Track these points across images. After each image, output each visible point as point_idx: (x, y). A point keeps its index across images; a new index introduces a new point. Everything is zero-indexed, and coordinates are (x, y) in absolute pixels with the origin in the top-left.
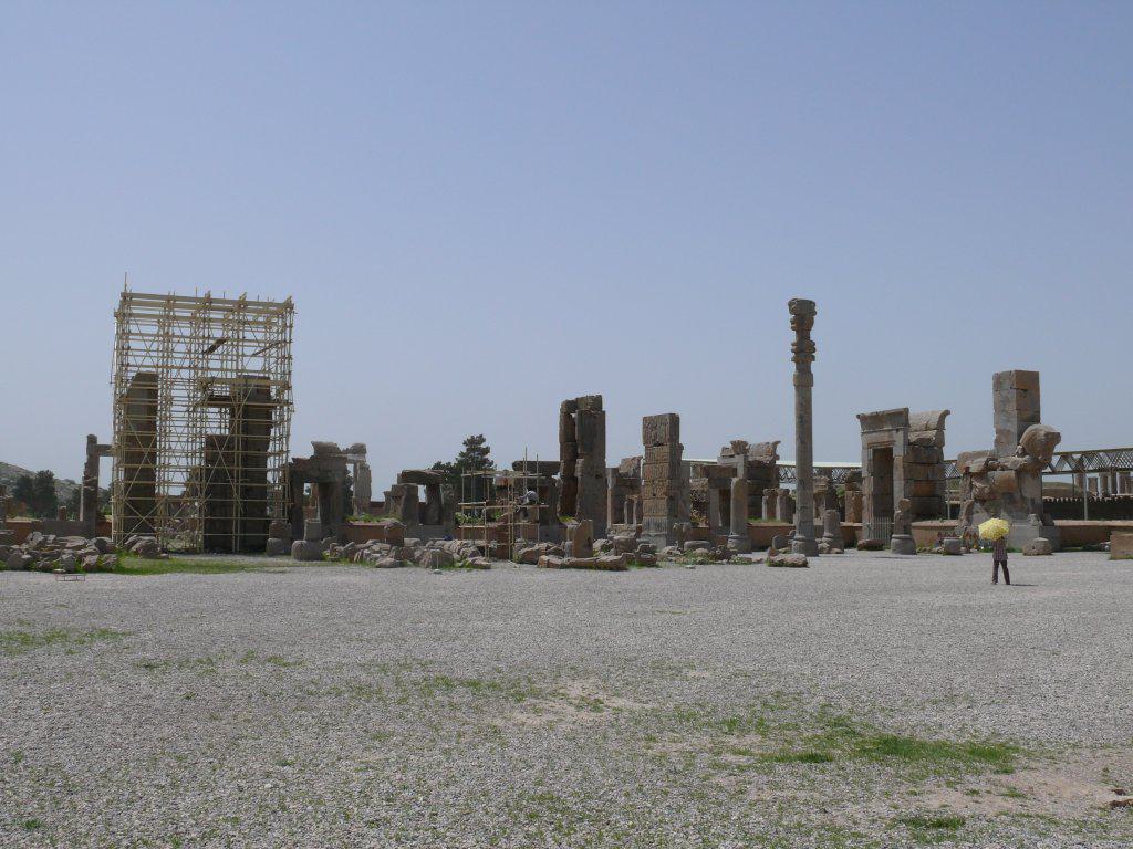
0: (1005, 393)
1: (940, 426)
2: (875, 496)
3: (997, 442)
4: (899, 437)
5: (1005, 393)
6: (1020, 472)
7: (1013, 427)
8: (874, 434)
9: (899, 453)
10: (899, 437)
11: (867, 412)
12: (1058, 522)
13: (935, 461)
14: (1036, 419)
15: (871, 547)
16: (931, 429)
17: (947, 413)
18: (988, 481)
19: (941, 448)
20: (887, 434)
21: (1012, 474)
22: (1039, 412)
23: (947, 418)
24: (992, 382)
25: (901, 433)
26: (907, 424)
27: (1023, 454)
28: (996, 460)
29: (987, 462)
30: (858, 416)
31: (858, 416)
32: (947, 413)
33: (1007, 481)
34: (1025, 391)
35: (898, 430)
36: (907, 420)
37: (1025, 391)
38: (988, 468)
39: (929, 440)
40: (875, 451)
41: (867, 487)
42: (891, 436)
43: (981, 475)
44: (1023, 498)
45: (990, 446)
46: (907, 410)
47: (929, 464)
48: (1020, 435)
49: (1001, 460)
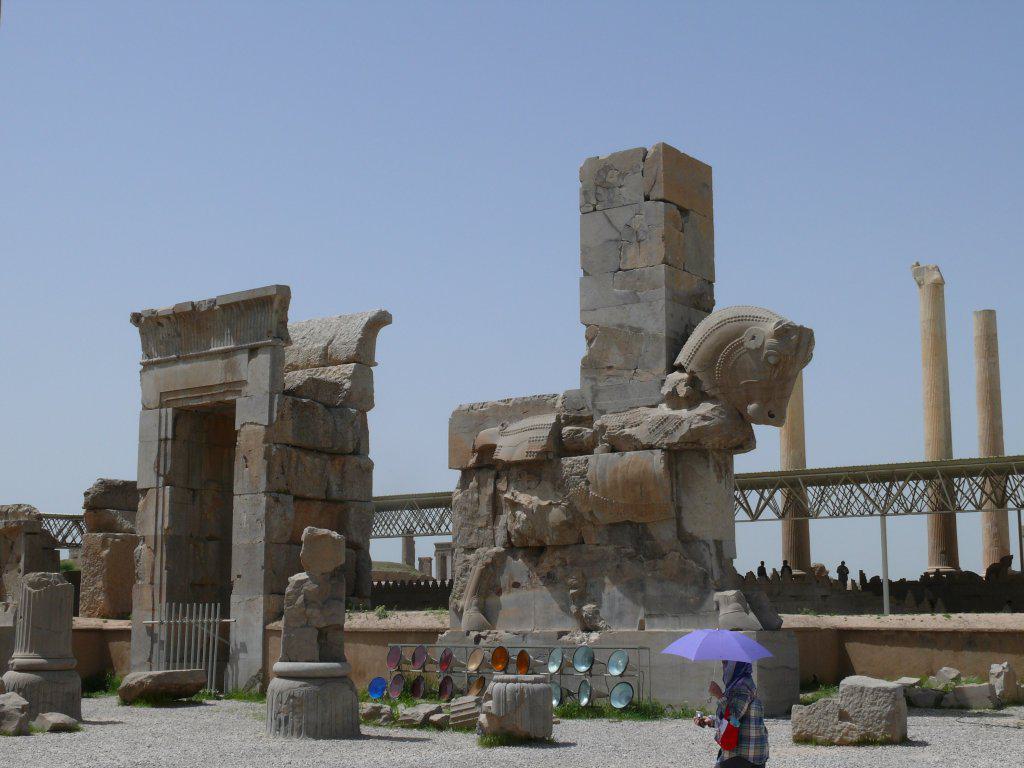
0: (621, 217)
1: (363, 356)
2: (174, 544)
3: (590, 366)
4: (256, 372)
5: (621, 217)
6: (683, 454)
7: (653, 319)
8: (181, 367)
9: (252, 416)
10: (256, 372)
11: (164, 303)
12: (790, 620)
13: (350, 447)
14: (701, 301)
15: (164, 695)
16: (337, 363)
17: (381, 320)
18: (559, 485)
19: (363, 413)
20: (220, 363)
21: (656, 461)
22: (711, 283)
23: (384, 333)
24: (576, 186)
25: (263, 359)
26: (282, 335)
27: (691, 402)
29: (557, 428)
30: (136, 319)
31: (136, 319)
32: (381, 320)
33: (636, 484)
34: (684, 212)
35: (253, 352)
37: (684, 212)
38: (561, 446)
39: (336, 387)
40: (179, 415)
41: (152, 519)
42: (232, 368)
43: (536, 469)
44: (685, 539)
46: (284, 293)
47: (333, 455)
48: (676, 342)
49: (611, 421)
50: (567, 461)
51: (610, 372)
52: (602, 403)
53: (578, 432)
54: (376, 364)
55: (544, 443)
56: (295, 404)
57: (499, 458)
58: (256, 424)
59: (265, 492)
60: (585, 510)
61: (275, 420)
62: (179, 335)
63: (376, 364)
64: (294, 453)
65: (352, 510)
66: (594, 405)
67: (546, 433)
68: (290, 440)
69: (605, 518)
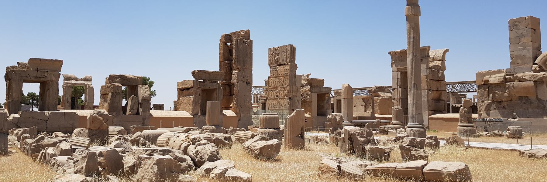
1: (443, 59)
28: (513, 75)
30: (390, 53)
31: (390, 53)
32: (447, 51)
36: (428, 53)
45: (509, 67)
50: (507, 83)
51: (518, 65)
52: (516, 71)
53: (510, 77)
54: (446, 60)
55: (502, 80)
56: (432, 71)
57: (491, 82)
58: (423, 75)
59: (427, 89)
60: (513, 93)
61: (428, 74)
62: (401, 56)
63: (446, 60)
64: (432, 81)
65: (443, 93)
66: (514, 72)
67: (503, 78)
68: (431, 79)
69: (518, 95)
